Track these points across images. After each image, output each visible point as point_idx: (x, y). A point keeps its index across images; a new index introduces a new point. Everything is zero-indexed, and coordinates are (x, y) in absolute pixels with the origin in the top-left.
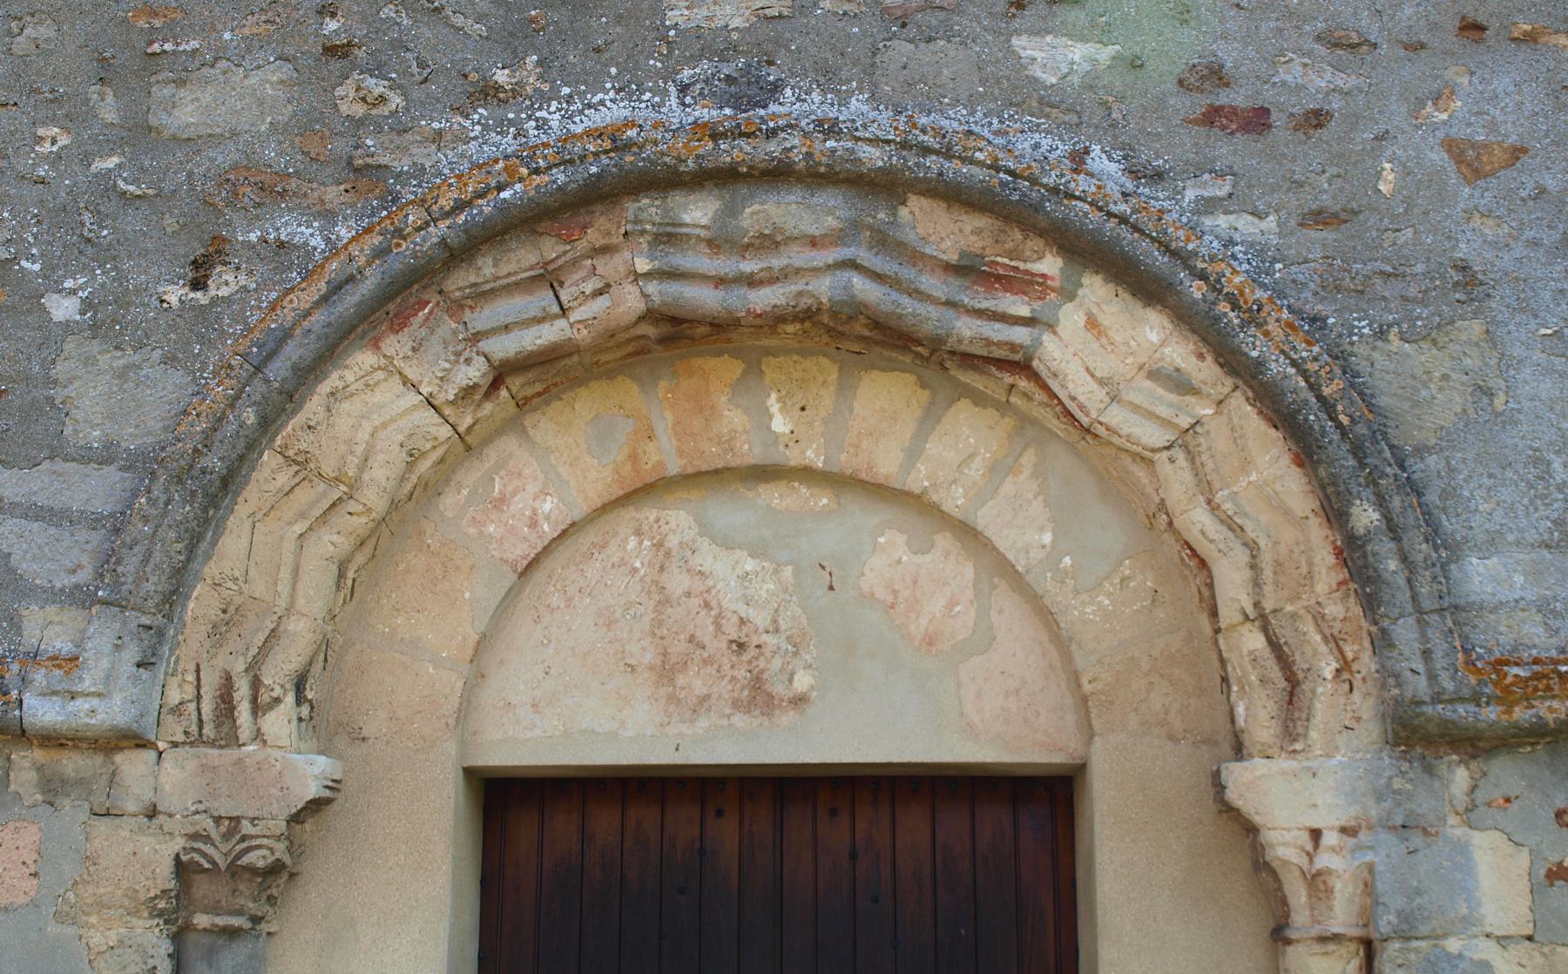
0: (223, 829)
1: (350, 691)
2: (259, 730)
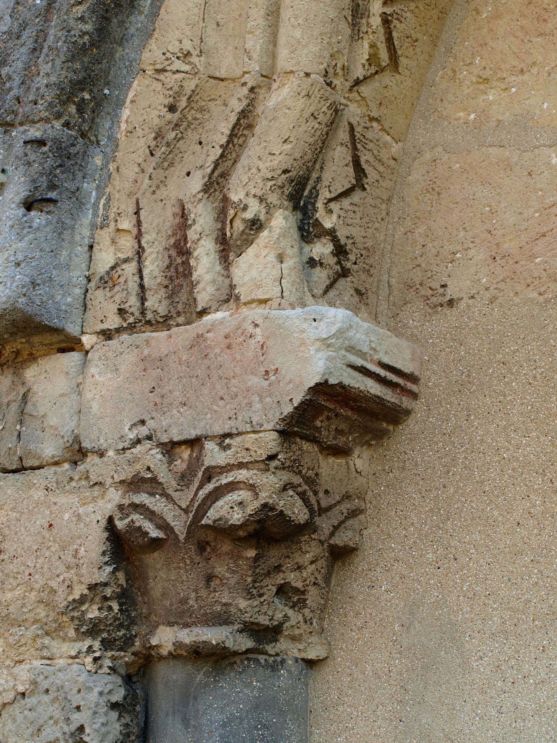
0: (180, 465)
1: (421, 230)
2: (232, 287)
